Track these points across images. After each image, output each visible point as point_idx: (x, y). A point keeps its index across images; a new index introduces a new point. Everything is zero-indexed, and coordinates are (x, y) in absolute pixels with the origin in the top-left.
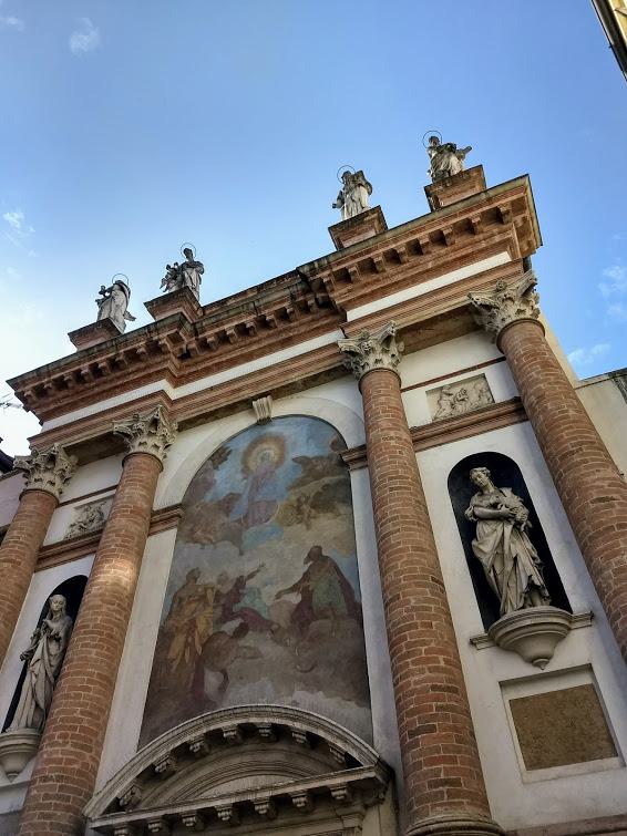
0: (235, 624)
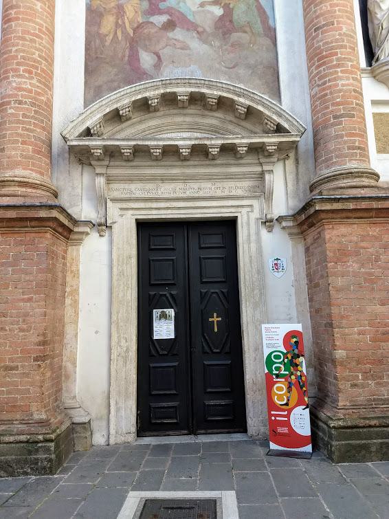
0: (160, 19)
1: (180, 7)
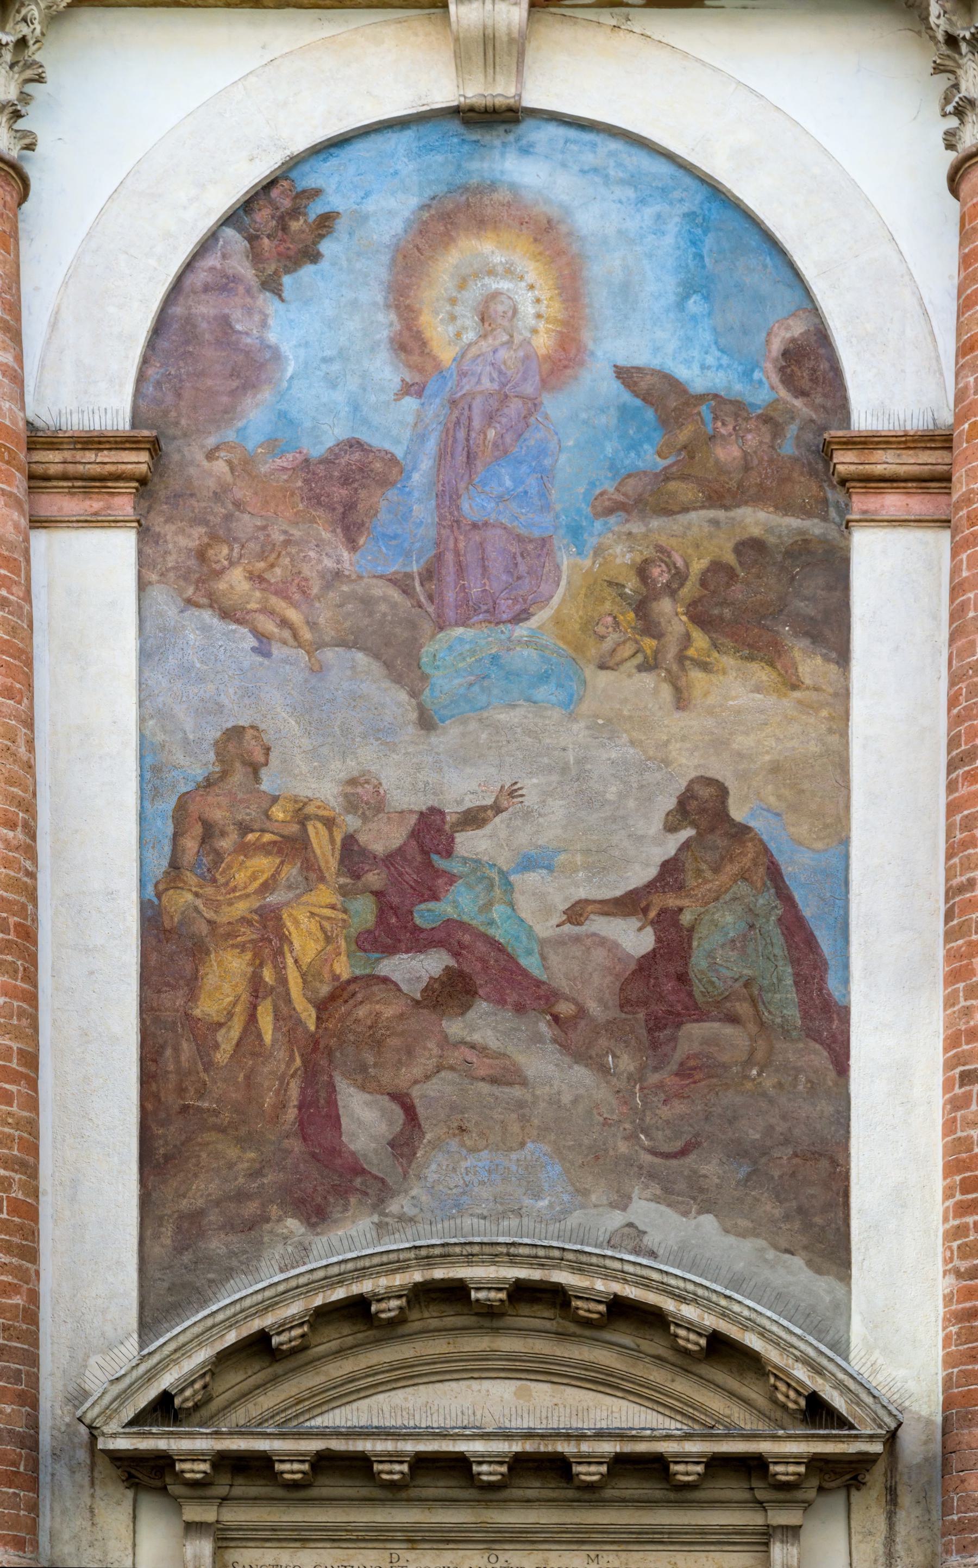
1: (491, 923)
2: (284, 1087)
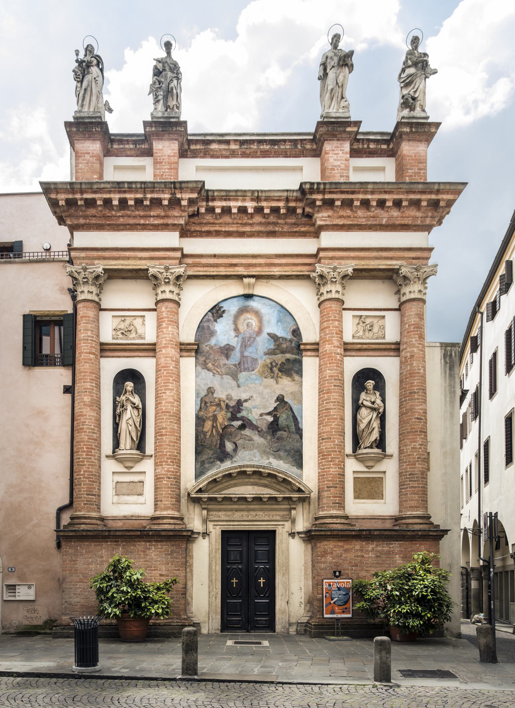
0: (237, 423)
2: (217, 442)
